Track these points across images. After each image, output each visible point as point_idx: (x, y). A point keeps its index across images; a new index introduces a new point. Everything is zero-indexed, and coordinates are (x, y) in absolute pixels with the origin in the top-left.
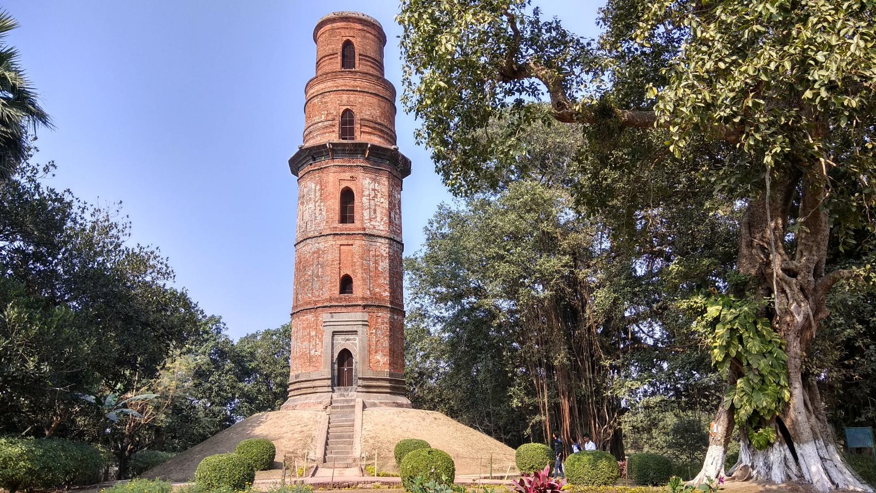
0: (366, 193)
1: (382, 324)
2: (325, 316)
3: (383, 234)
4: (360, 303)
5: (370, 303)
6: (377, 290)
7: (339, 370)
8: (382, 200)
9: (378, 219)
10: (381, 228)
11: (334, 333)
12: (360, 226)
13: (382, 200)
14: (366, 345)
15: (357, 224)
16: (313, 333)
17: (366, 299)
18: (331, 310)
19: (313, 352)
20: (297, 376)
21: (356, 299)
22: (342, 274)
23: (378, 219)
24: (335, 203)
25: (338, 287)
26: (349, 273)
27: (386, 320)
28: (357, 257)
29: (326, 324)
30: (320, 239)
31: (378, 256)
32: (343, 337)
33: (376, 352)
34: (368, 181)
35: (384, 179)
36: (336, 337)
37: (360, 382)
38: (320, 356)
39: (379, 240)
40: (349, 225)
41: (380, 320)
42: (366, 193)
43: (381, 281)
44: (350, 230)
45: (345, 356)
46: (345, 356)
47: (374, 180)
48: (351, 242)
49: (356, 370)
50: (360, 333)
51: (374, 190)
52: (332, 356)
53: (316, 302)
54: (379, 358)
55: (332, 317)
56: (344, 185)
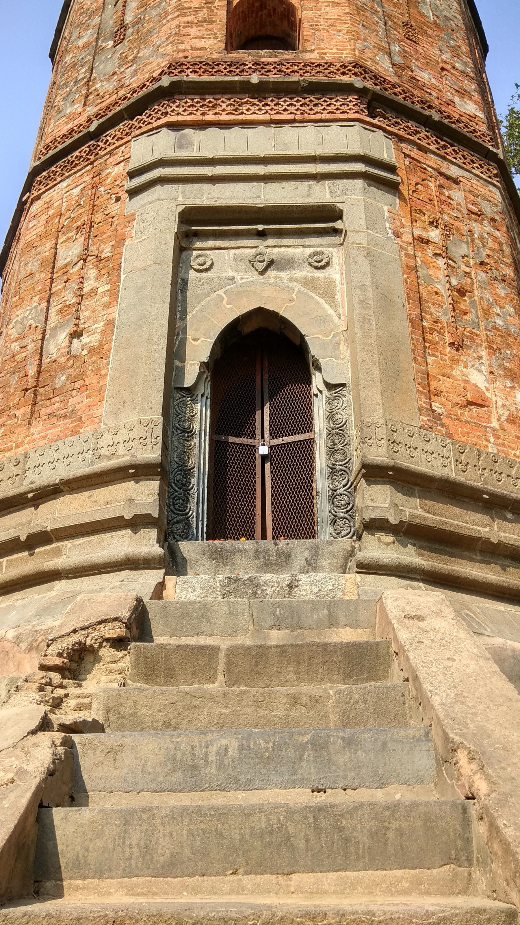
2: (145, 147)
7: (219, 452)
16: (70, 251)
18: (180, 111)
19: (57, 345)
25: (219, 27)
29: (144, 180)
32: (248, 248)
33: (457, 346)
36: (204, 252)
37: (379, 500)
38: (99, 352)
41: (457, 195)
45: (263, 358)
49: (337, 431)
50: (353, 221)
52: (175, 351)
54: (478, 379)
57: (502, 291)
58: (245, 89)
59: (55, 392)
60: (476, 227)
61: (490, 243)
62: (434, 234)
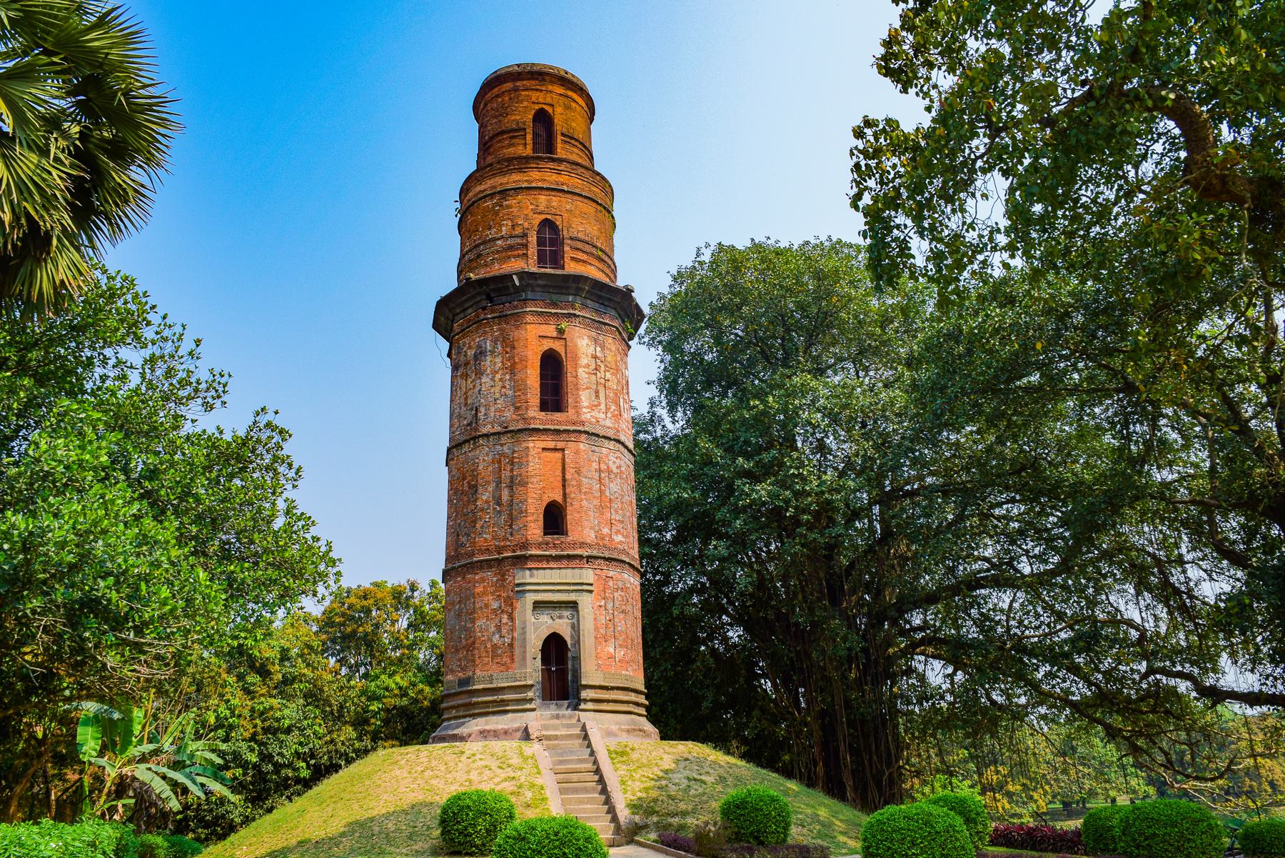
0: (584, 361)
3: (610, 434)
4: (579, 552)
5: (595, 553)
6: (606, 531)
10: (608, 423)
11: (538, 605)
12: (574, 418)
15: (571, 411)
17: (590, 546)
20: (465, 682)
21: (574, 545)
22: (546, 500)
23: (603, 407)
24: (532, 377)
25: (541, 523)
26: (559, 499)
27: (620, 584)
28: (572, 471)
30: (503, 439)
35: (610, 340)
39: (606, 442)
40: (557, 416)
41: (611, 583)
44: (559, 423)
46: (555, 649)
47: (596, 341)
48: (560, 445)
51: (595, 357)
53: (499, 550)
55: (531, 576)
56: (547, 345)
57: (622, 616)
58: (551, 556)
59: (497, 656)
62: (603, 603)
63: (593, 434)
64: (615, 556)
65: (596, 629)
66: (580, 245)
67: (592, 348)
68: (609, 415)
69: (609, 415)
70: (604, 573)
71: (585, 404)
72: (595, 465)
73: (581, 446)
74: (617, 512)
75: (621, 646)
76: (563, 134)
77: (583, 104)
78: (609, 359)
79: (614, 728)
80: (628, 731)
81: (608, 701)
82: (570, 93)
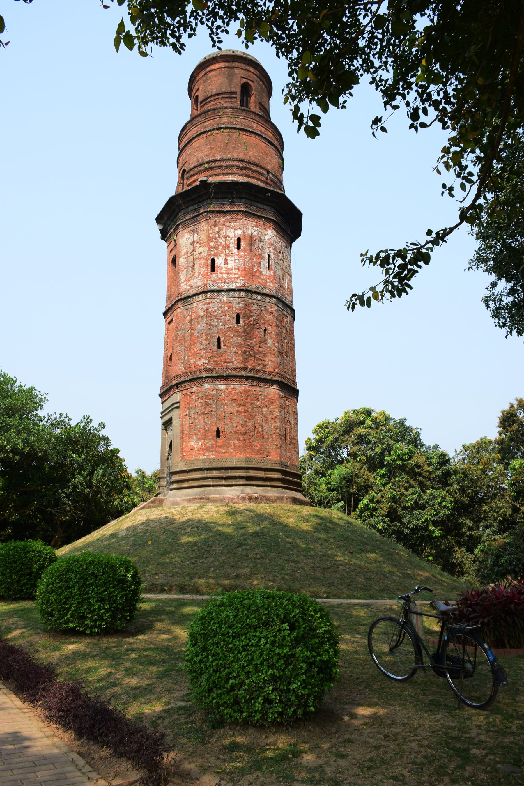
1: (197, 400)
5: (182, 379)
6: (193, 361)
8: (201, 249)
9: (196, 274)
10: (200, 283)
13: (201, 249)
14: (179, 431)
17: (179, 376)
27: (200, 395)
31: (195, 318)
33: (189, 438)
34: (186, 236)
35: (203, 224)
41: (194, 397)
42: (184, 251)
43: (198, 347)
54: (193, 444)
57: (201, 417)
60: (197, 403)
61: (200, 405)
63: (186, 298)
64: (198, 375)
65: (182, 432)
66: (192, 172)
67: (191, 238)
68: (200, 277)
69: (200, 277)
70: (187, 392)
71: (182, 281)
72: (188, 318)
73: (179, 310)
74: (201, 343)
75: (199, 439)
76: (201, 102)
77: (222, 65)
78: (202, 237)
79: (178, 499)
80: (189, 501)
81: (188, 480)
82: (208, 69)
